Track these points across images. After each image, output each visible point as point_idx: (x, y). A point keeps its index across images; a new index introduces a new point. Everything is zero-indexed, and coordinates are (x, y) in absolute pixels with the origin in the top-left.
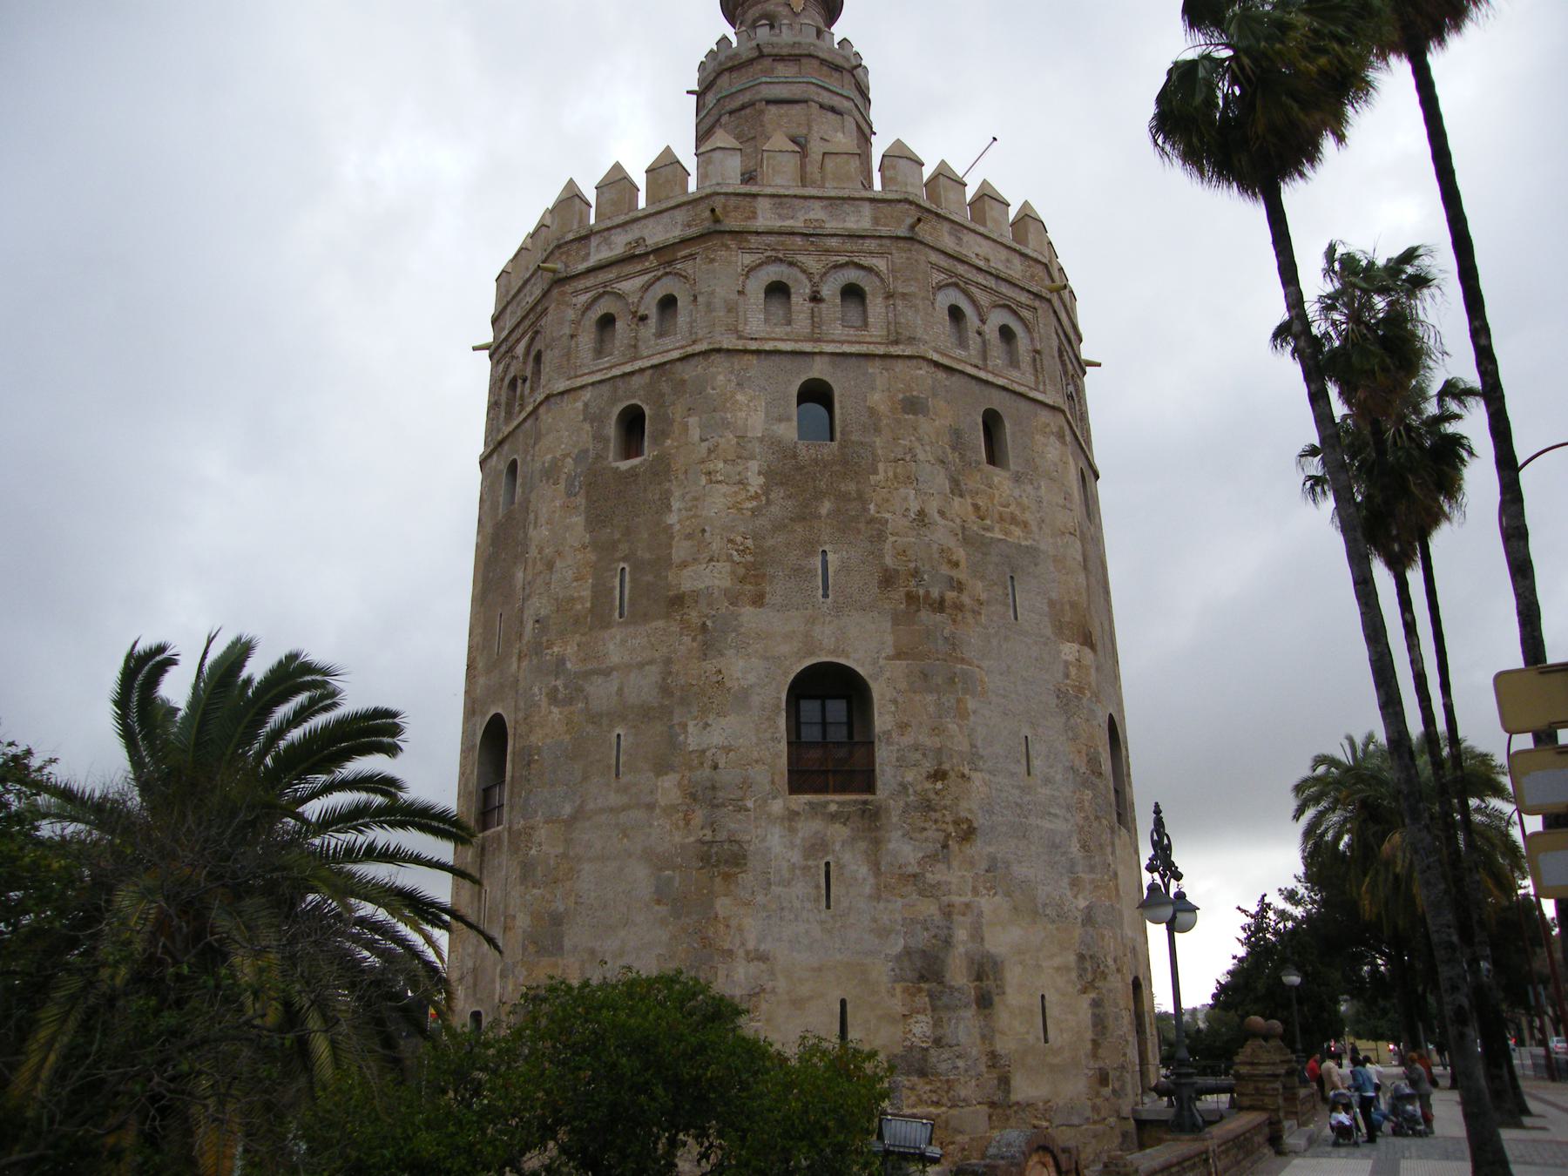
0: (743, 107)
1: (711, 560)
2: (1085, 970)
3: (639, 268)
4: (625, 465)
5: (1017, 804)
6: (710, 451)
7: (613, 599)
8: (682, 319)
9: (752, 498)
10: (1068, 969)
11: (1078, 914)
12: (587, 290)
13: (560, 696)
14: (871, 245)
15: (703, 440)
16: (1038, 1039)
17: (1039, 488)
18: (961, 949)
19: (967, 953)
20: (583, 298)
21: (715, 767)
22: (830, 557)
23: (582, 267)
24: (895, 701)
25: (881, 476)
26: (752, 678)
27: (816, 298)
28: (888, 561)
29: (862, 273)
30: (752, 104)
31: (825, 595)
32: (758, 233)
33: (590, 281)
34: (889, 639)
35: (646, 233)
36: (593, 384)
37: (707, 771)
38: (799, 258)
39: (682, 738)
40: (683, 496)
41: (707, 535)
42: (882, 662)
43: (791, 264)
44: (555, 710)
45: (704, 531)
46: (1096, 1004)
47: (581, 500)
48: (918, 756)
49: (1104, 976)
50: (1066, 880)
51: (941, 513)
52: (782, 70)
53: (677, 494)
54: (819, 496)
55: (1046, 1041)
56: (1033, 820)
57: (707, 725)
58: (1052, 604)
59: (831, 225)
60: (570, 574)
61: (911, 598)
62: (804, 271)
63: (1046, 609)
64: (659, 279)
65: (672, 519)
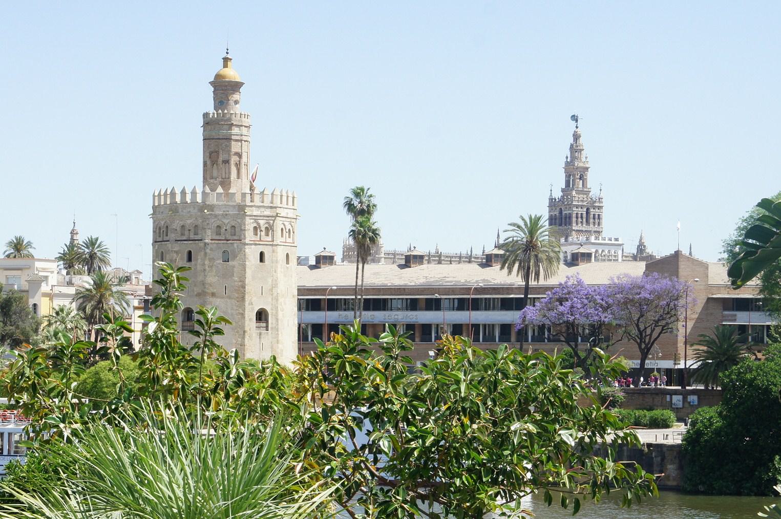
4: (288, 265)
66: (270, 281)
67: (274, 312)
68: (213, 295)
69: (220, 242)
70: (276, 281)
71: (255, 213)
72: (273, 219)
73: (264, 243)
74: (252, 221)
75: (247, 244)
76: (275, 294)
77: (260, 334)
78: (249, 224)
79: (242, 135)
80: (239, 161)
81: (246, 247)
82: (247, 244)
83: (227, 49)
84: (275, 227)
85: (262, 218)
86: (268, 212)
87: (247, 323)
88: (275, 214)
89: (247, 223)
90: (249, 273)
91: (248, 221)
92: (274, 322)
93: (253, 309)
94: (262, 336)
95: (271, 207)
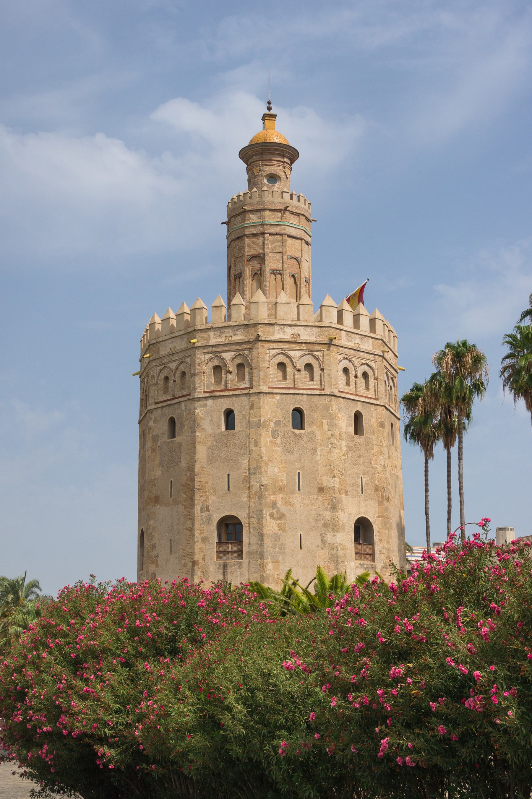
0: (276, 234)
1: (334, 477)
3: (298, 348)
4: (297, 432)
6: (332, 435)
7: (295, 483)
8: (316, 376)
9: (344, 455)
12: (274, 349)
13: (275, 516)
14: (371, 357)
15: (329, 430)
20: (273, 352)
21: (338, 550)
22: (363, 479)
23: (272, 338)
24: (379, 532)
25: (374, 451)
26: (345, 521)
27: (356, 377)
28: (377, 482)
29: (368, 368)
30: (282, 235)
31: (362, 493)
32: (342, 347)
33: (275, 345)
34: (377, 510)
35: (300, 333)
36: (281, 394)
37: (335, 552)
38: (353, 359)
39: (325, 539)
40: (322, 450)
41: (332, 467)
42: (376, 518)
43: (350, 361)
44: (273, 521)
45: (331, 465)
47: (279, 440)
48: (384, 550)
52: (293, 220)
53: (319, 449)
54: (359, 457)
57: (334, 536)
59: (362, 347)
60: (276, 470)
61: (382, 496)
62: (353, 365)
64: (305, 355)
65: (318, 457)
66: (246, 462)
67: (254, 521)
68: (157, 500)
69: (164, 404)
70: (257, 460)
71: (212, 342)
72: (248, 346)
73: (231, 393)
74: (208, 356)
75: (199, 399)
76: (256, 487)
77: (225, 566)
78: (204, 363)
79: (263, 225)
80: (261, 270)
81: (197, 404)
82: (199, 399)
83: (269, 103)
84: (254, 361)
85: (227, 348)
86: (239, 337)
87: (198, 546)
88: (252, 338)
89: (197, 361)
90: (201, 452)
91: (202, 357)
92: (254, 540)
93: (209, 519)
94: (229, 571)
95: (246, 326)
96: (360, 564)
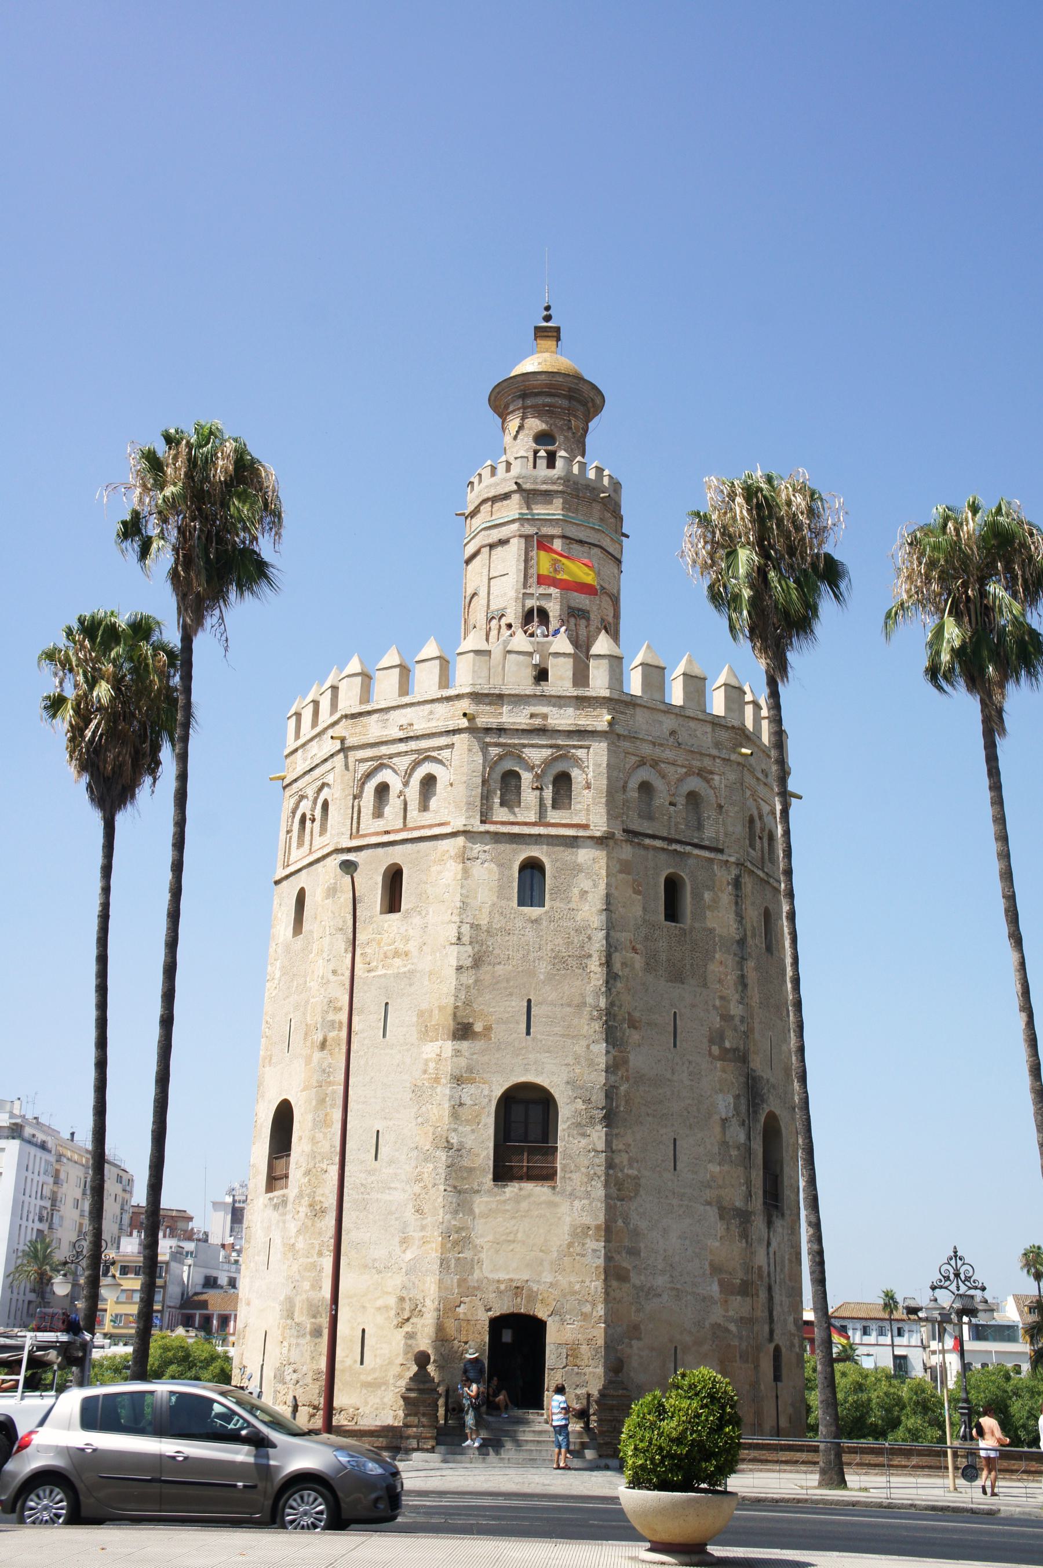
2: (403, 1309)
5: (362, 1185)
10: (387, 1308)
11: (403, 1265)
16: (355, 1361)
17: (427, 914)
18: (304, 1296)
19: (308, 1299)
46: (410, 1336)
49: (421, 1314)
50: (397, 1239)
51: (334, 972)
55: (362, 1363)
56: (374, 1195)
58: (421, 1014)
63: (415, 1019)
96: (270, 1199)
